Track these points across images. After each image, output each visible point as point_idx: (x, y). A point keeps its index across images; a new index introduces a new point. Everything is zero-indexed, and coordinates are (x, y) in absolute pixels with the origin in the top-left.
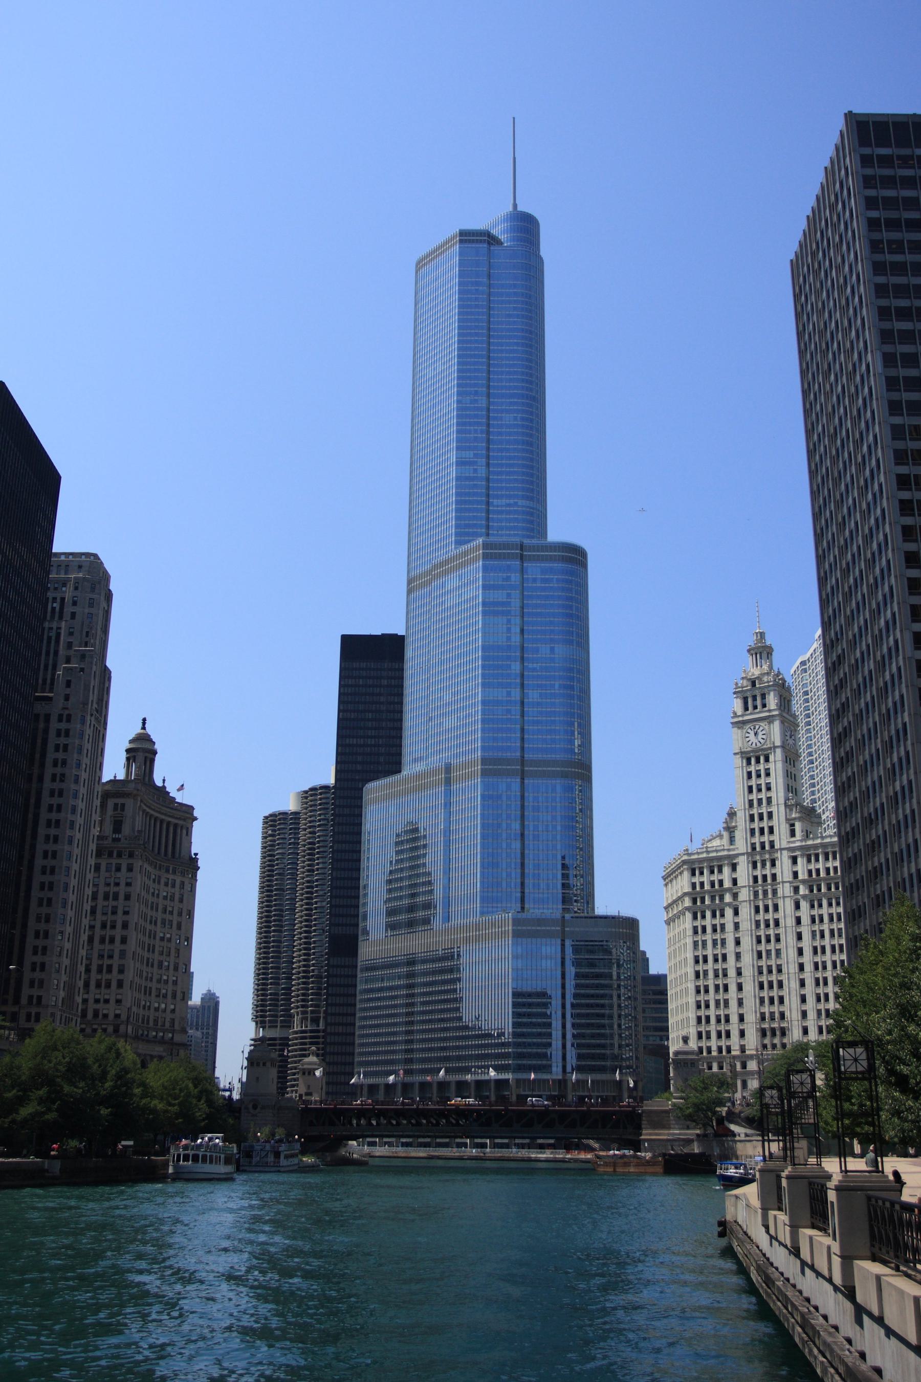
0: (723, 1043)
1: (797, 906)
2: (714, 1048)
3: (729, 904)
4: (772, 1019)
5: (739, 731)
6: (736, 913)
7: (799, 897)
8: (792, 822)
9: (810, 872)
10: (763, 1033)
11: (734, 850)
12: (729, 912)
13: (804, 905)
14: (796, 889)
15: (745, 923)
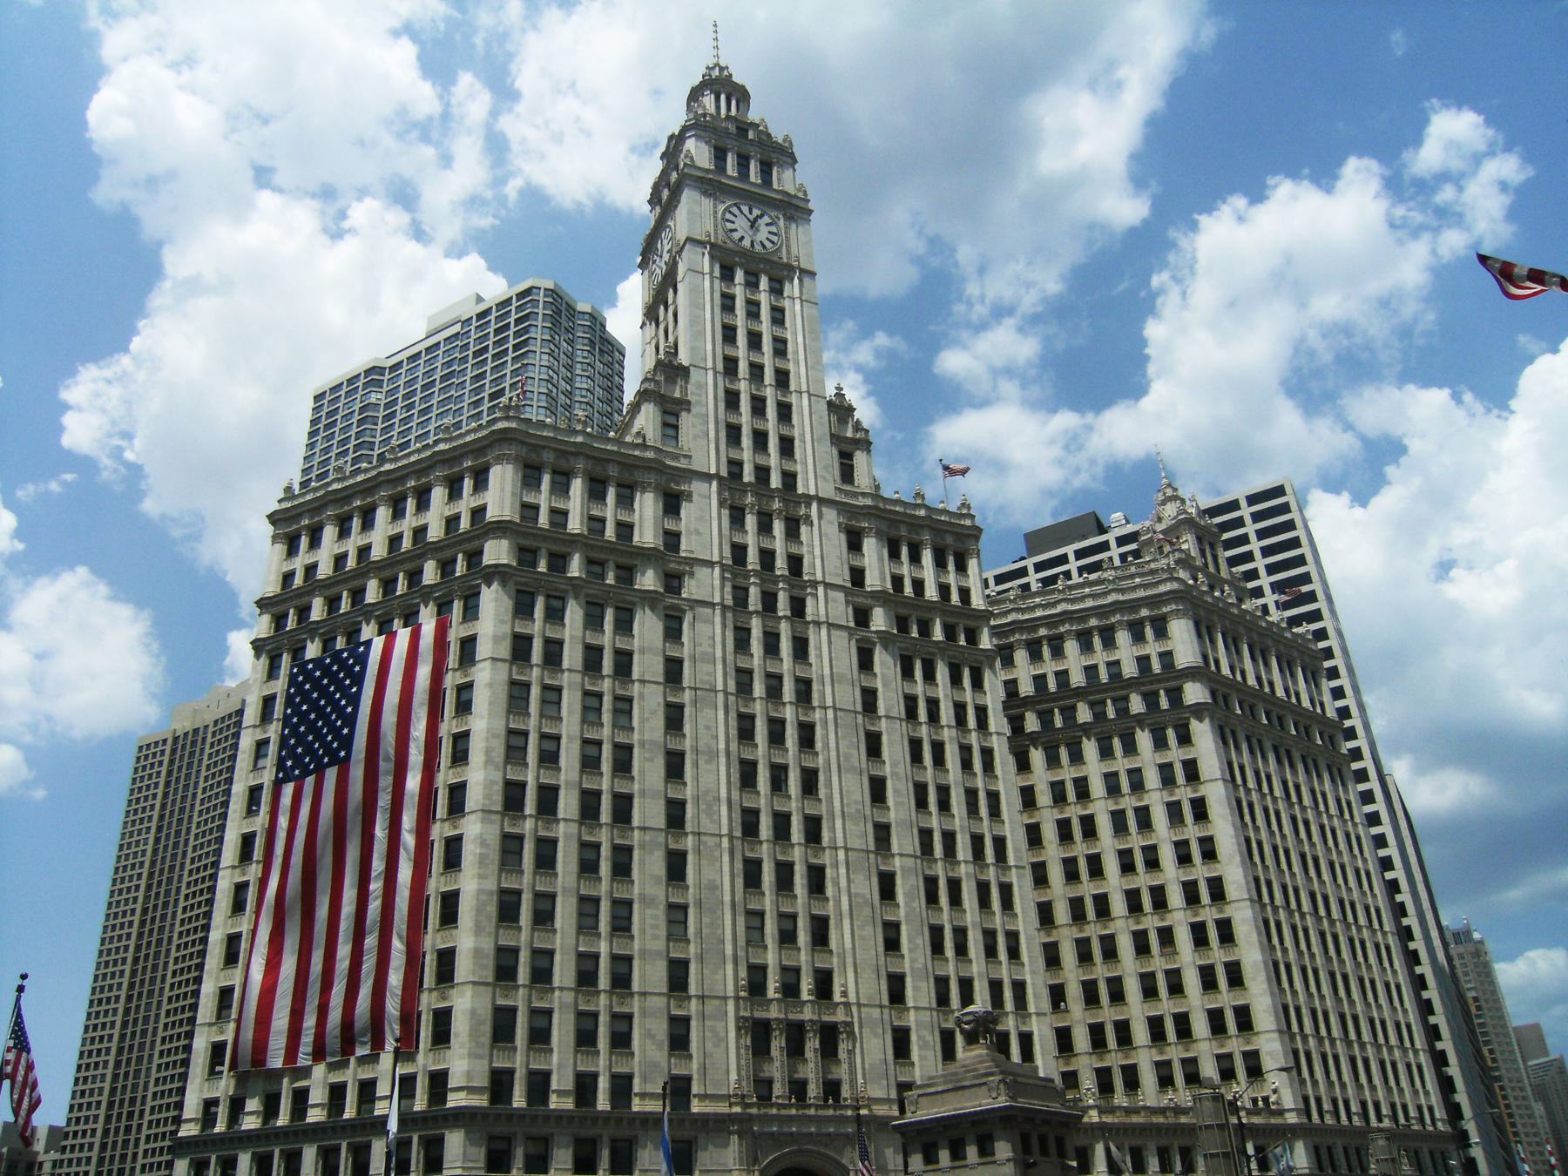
1: (865, 663)
2: (562, 1080)
3: (650, 599)
6: (673, 633)
8: (846, 448)
9: (897, 581)
10: (758, 1034)
11: (676, 457)
12: (647, 626)
13: (884, 662)
14: (862, 617)
15: (704, 668)
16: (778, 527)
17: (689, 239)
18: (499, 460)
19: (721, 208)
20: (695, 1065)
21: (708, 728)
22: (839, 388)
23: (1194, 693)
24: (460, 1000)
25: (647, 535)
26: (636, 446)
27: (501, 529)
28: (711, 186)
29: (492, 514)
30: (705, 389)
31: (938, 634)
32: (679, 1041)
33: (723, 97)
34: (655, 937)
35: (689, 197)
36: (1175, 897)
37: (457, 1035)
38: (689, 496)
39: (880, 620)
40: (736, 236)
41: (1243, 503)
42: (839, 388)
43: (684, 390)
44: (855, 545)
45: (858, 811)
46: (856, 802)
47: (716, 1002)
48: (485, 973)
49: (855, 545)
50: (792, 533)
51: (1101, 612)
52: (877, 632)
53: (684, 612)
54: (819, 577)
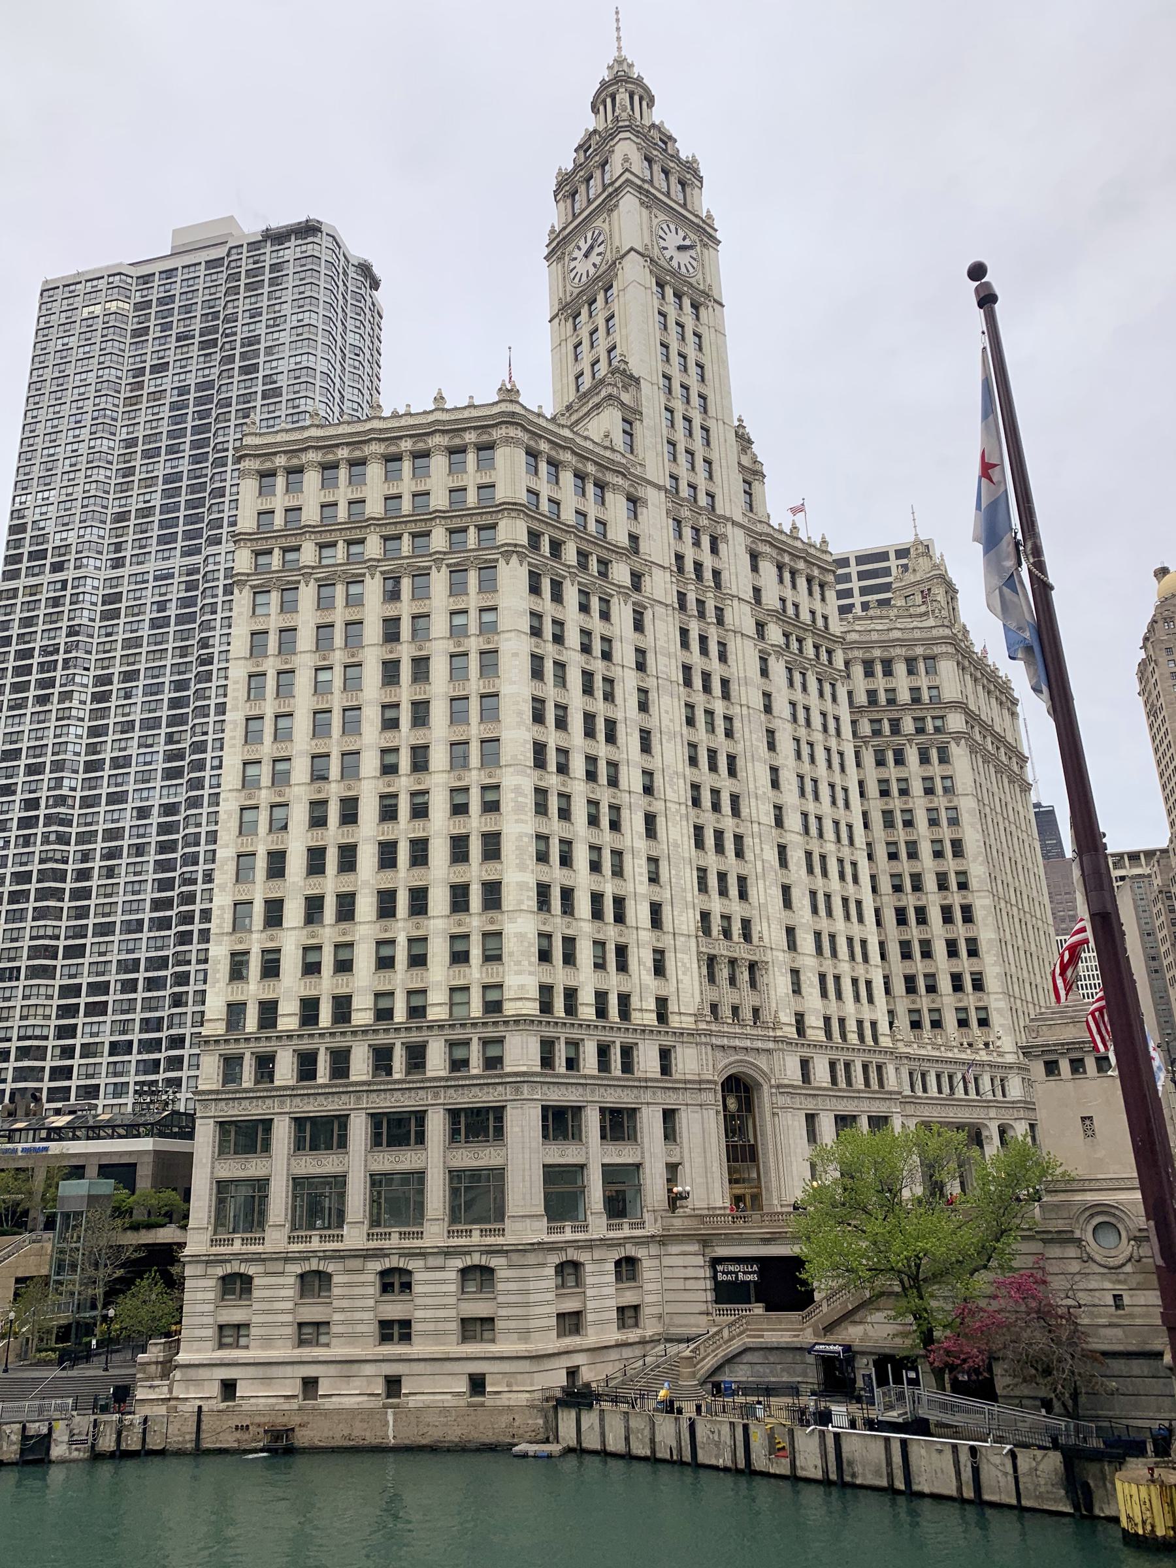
0: (613, 982)
2: (586, 997)
4: (727, 933)
5: (645, 212)
7: (770, 649)
13: (777, 668)
16: (705, 541)
17: (632, 249)
18: (508, 441)
19: (655, 221)
20: (673, 989)
21: (667, 712)
22: (740, 420)
23: (955, 722)
24: (511, 925)
25: (619, 535)
26: (606, 448)
27: (512, 508)
28: (649, 200)
29: (502, 494)
30: (651, 399)
31: (810, 651)
32: (659, 969)
33: (636, 98)
34: (641, 883)
35: (629, 203)
36: (930, 883)
37: (511, 954)
38: (645, 503)
39: (774, 634)
40: (668, 254)
41: (892, 556)
42: (740, 420)
43: (637, 400)
44: (755, 568)
45: (764, 793)
46: (763, 786)
47: (682, 939)
48: (531, 903)
49: (755, 568)
50: (714, 550)
51: (885, 645)
52: (772, 645)
53: (645, 608)
54: (734, 592)
